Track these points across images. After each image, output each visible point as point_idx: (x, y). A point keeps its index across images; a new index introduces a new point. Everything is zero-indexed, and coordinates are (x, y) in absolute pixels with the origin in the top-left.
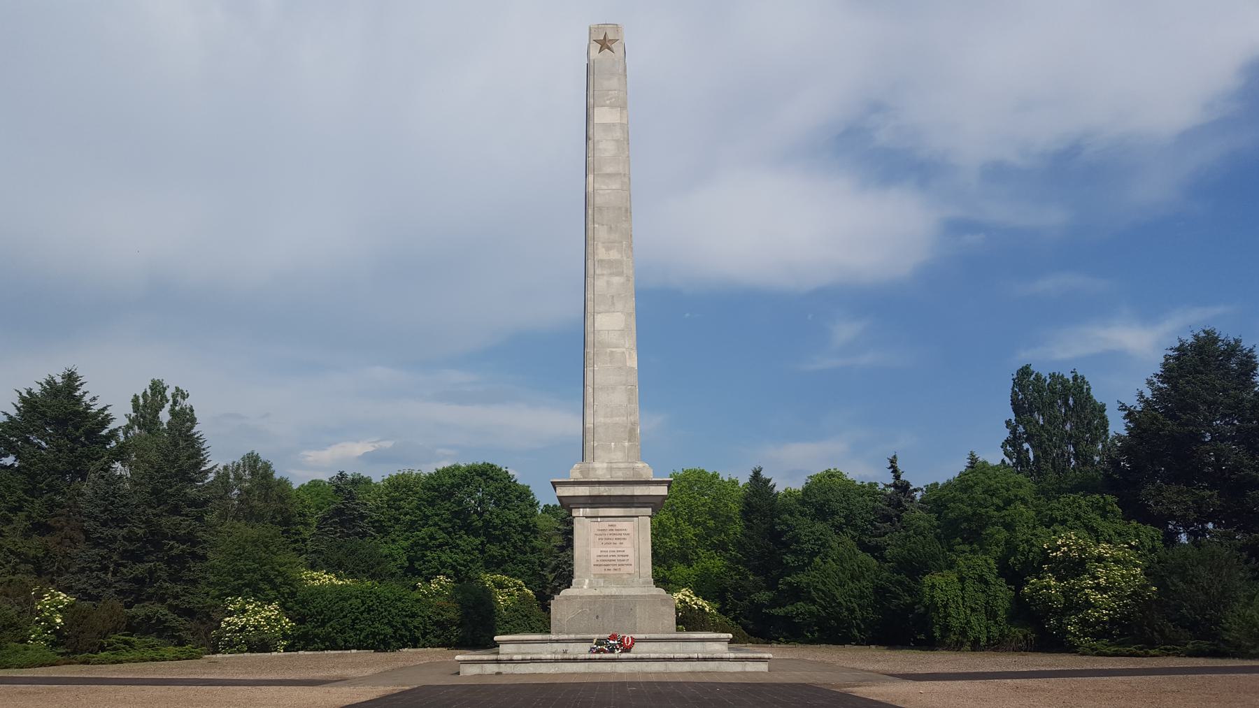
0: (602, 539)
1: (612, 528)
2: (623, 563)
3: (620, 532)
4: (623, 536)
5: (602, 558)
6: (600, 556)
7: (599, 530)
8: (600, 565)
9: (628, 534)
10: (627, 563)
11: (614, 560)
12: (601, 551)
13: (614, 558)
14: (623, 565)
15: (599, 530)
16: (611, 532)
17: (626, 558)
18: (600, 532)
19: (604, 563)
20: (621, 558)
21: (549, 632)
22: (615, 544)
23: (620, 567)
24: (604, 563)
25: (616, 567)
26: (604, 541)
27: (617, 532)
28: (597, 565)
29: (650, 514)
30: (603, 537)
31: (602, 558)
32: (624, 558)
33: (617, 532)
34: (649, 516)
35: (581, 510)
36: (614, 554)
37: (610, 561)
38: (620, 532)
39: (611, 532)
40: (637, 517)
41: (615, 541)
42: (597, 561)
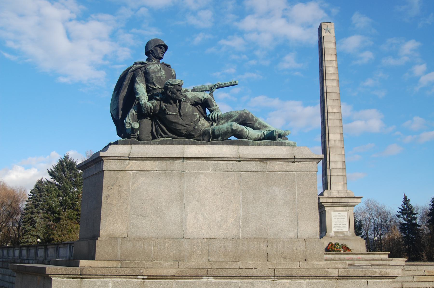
0: (336, 218)
1: (339, 214)
3: (342, 216)
4: (344, 218)
6: (335, 225)
8: (336, 228)
9: (345, 217)
10: (345, 227)
12: (336, 223)
13: (340, 225)
14: (344, 228)
16: (339, 216)
17: (345, 225)
18: (335, 216)
19: (337, 227)
20: (343, 225)
22: (341, 220)
23: (343, 229)
24: (337, 227)
25: (341, 229)
27: (341, 216)
28: (334, 228)
30: (336, 218)
33: (341, 216)
36: (340, 224)
37: (339, 226)
38: (342, 216)
39: (339, 216)
42: (335, 226)
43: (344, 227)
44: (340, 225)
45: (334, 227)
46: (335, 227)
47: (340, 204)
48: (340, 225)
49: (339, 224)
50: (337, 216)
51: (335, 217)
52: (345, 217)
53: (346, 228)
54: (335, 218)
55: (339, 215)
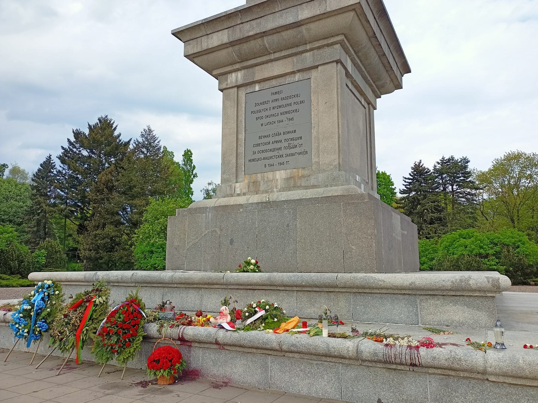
0: (262, 118)
2: (293, 151)
4: (294, 107)
5: (262, 148)
6: (258, 145)
8: (258, 160)
9: (302, 102)
11: (280, 149)
12: (260, 138)
14: (293, 155)
16: (276, 104)
21: (164, 269)
25: (281, 160)
27: (284, 102)
31: (262, 148)
32: (296, 143)
33: (284, 102)
35: (234, 74)
36: (277, 138)
37: (274, 150)
39: (276, 104)
40: (317, 67)
41: (280, 117)
42: (254, 153)
43: (293, 151)
44: (276, 142)
46: (257, 156)
47: (267, 41)
48: (276, 142)
49: (271, 139)
52: (302, 102)
53: (300, 154)
54: (257, 119)
55: (276, 100)
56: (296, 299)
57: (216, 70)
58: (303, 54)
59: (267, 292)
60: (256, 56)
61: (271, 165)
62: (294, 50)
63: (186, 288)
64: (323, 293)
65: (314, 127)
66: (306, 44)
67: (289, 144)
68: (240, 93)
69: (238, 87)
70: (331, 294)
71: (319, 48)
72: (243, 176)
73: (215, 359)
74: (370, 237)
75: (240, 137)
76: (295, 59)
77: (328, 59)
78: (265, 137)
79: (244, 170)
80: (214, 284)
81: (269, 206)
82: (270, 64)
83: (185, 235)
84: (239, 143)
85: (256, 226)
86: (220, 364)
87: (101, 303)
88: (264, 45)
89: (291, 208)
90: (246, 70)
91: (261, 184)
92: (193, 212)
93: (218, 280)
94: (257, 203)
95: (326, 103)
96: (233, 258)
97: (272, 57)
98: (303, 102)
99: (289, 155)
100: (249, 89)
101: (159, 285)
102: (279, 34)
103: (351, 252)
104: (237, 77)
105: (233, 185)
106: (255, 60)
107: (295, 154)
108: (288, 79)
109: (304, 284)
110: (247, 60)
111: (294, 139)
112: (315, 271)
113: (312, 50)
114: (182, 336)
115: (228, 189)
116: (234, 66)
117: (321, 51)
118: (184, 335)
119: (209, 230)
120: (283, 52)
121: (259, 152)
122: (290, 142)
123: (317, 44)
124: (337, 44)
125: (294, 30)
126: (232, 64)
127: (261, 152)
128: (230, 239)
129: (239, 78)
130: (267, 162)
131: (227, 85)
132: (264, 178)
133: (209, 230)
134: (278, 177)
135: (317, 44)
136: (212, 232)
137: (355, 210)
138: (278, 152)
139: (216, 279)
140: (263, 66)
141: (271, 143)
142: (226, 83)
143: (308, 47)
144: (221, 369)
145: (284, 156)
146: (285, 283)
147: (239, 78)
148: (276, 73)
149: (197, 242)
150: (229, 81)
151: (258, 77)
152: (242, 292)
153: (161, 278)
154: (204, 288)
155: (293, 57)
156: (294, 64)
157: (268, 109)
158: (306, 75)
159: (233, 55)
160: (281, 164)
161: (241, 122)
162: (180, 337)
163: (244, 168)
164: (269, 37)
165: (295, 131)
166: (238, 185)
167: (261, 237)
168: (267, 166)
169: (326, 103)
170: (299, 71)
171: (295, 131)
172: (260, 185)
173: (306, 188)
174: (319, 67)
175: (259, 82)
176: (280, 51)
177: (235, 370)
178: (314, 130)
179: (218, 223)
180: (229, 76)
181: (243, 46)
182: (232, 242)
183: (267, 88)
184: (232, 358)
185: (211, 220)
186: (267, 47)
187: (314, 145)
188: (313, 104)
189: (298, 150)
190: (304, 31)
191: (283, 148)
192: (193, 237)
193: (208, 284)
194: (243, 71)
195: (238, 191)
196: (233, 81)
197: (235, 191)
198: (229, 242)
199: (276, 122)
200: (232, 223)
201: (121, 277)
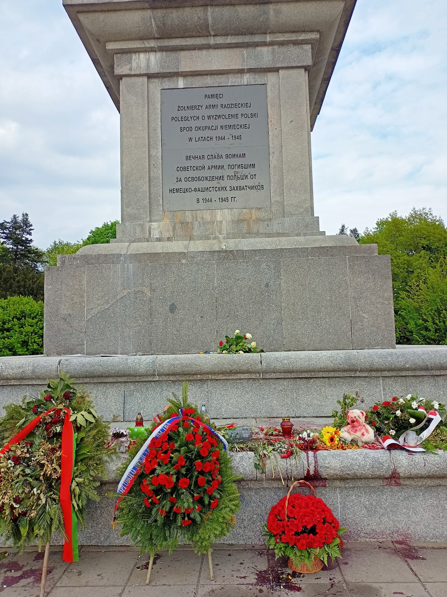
0: (190, 129)
2: (241, 183)
3: (234, 111)
4: (242, 121)
5: (191, 174)
6: (185, 169)
7: (180, 108)
8: (186, 191)
9: (254, 115)
11: (221, 178)
12: (188, 158)
15: (180, 108)
16: (212, 112)
25: (223, 194)
26: (195, 134)
27: (226, 112)
28: (177, 190)
29: (309, 62)
31: (191, 174)
33: (226, 112)
34: (306, 68)
35: (142, 55)
37: (212, 178)
38: (234, 111)
39: (212, 112)
40: (276, 70)
41: (220, 133)
43: (241, 183)
44: (215, 167)
45: (178, 186)
46: (184, 185)
48: (215, 167)
49: (207, 163)
50: (195, 113)
51: (187, 119)
52: (254, 115)
53: (252, 188)
54: (182, 129)
55: (214, 106)
56: (384, 389)
57: (112, 43)
58: (257, 48)
59: (332, 381)
60: (187, 34)
61: (206, 200)
62: (247, 39)
63: (173, 382)
64: (426, 378)
65: (273, 153)
66: (265, 33)
67: (235, 172)
68: (151, 86)
69: (150, 76)
70: (439, 379)
71: (282, 44)
72: (161, 213)
73: (371, 504)
74: (387, 302)
75: (153, 153)
76: (245, 51)
77: (295, 61)
78: (195, 158)
79: (161, 203)
80: (237, 373)
81: (232, 258)
82: (204, 52)
83: (82, 297)
84: (152, 162)
85: (216, 285)
86: (382, 511)
87: (91, 423)
88: (206, 20)
89: (271, 261)
90: (164, 53)
91: (195, 227)
92: (92, 261)
93: (251, 366)
94: (210, 252)
95: (291, 122)
96: (175, 332)
97: (212, 41)
98: (256, 115)
99: (236, 188)
100: (167, 84)
101: (119, 380)
102: (232, 8)
103: (362, 321)
104: (148, 60)
105: (147, 225)
106: (184, 40)
107: (245, 187)
108: (232, 80)
109: (407, 366)
110: (170, 37)
111: (243, 166)
112: (311, 348)
113: (272, 44)
114: (316, 471)
115: (138, 229)
116: (146, 42)
117: (284, 49)
118: (320, 469)
119: (130, 291)
120: (229, 37)
121: (187, 179)
122: (236, 170)
123: (281, 38)
124: (308, 44)
125: (258, 7)
126: (142, 39)
127: (190, 179)
128: (169, 304)
129: (153, 63)
130: (201, 195)
131: (131, 69)
132: (196, 219)
133: (130, 291)
134: (219, 218)
135: (281, 38)
136: (136, 293)
137: (366, 267)
138: (218, 183)
139: (248, 363)
140: (193, 52)
141: (206, 168)
142: (129, 66)
143: (268, 38)
144: (385, 519)
145: (228, 189)
146: (376, 366)
147: (153, 63)
148: (215, 67)
149: (108, 309)
150: (134, 65)
151: (184, 67)
152: (285, 382)
153: (130, 367)
154: (212, 380)
155: (242, 49)
156: (244, 58)
157: (200, 118)
158: (259, 79)
159: (151, 24)
160: (225, 200)
161: (155, 130)
162: (312, 473)
163: (161, 201)
164: (217, 9)
165: (244, 155)
166: (155, 225)
167: (223, 301)
168: (201, 201)
169: (291, 122)
170: (250, 71)
171: (244, 155)
172: (193, 228)
173: (269, 235)
174: (280, 71)
175: (185, 75)
176: (224, 36)
177: (415, 518)
178: (273, 157)
179: (147, 281)
180: (134, 56)
181: (172, 13)
182: (173, 308)
183: (197, 86)
184: (405, 499)
185: (134, 275)
186: (210, 24)
187: (274, 178)
188: (271, 121)
189: (249, 182)
190: (272, 13)
191: (225, 178)
192: (98, 300)
193: (231, 372)
194: (159, 54)
195: (156, 234)
196: (142, 66)
197: (150, 234)
198: (167, 308)
199: (214, 139)
200: (172, 281)
201: (31, 368)
